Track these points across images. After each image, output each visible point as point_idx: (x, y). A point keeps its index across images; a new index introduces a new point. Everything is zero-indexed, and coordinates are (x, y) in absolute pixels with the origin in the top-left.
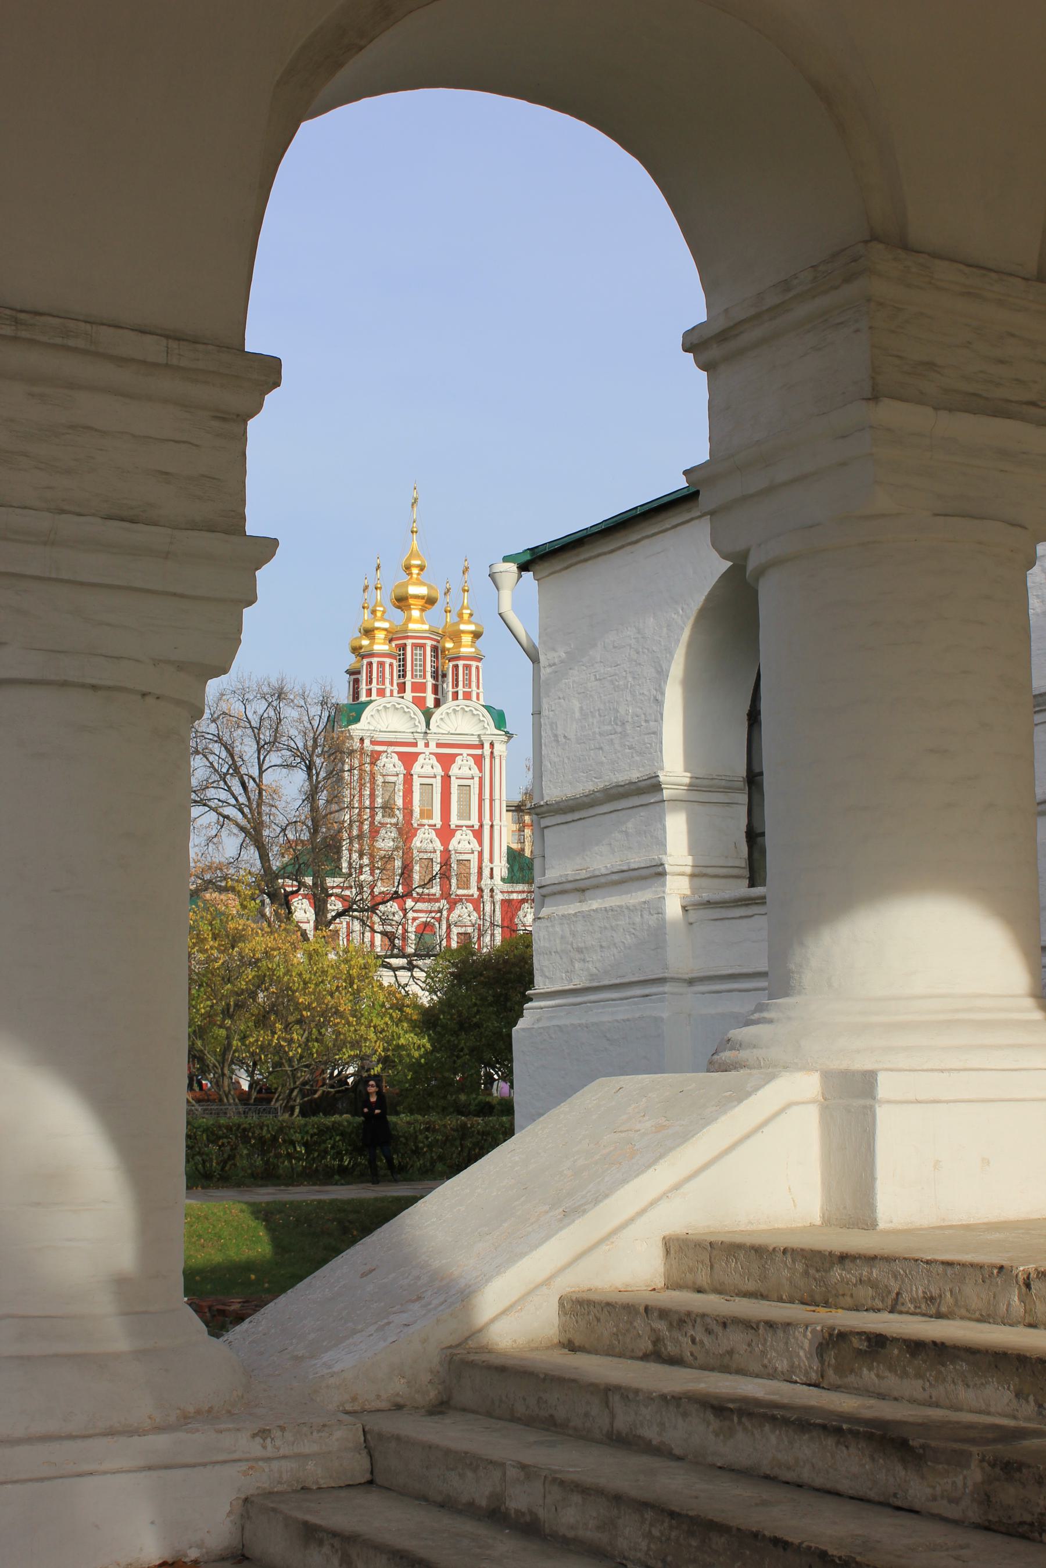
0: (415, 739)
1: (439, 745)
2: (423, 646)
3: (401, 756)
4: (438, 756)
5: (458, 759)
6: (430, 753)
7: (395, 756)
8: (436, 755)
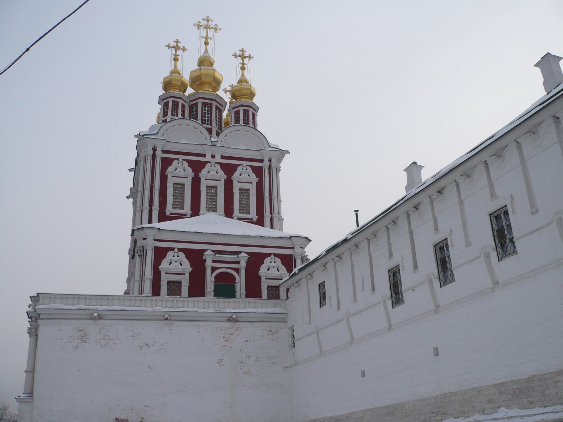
0: (204, 150)
1: (223, 157)
2: (211, 105)
3: (191, 164)
4: (223, 166)
5: (239, 168)
6: (216, 163)
7: (186, 164)
8: (220, 164)
